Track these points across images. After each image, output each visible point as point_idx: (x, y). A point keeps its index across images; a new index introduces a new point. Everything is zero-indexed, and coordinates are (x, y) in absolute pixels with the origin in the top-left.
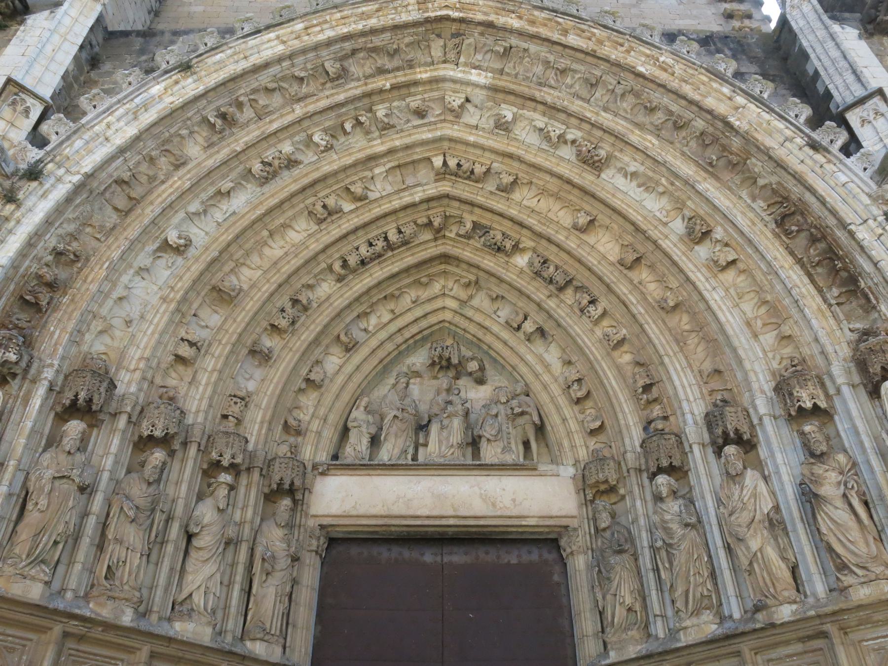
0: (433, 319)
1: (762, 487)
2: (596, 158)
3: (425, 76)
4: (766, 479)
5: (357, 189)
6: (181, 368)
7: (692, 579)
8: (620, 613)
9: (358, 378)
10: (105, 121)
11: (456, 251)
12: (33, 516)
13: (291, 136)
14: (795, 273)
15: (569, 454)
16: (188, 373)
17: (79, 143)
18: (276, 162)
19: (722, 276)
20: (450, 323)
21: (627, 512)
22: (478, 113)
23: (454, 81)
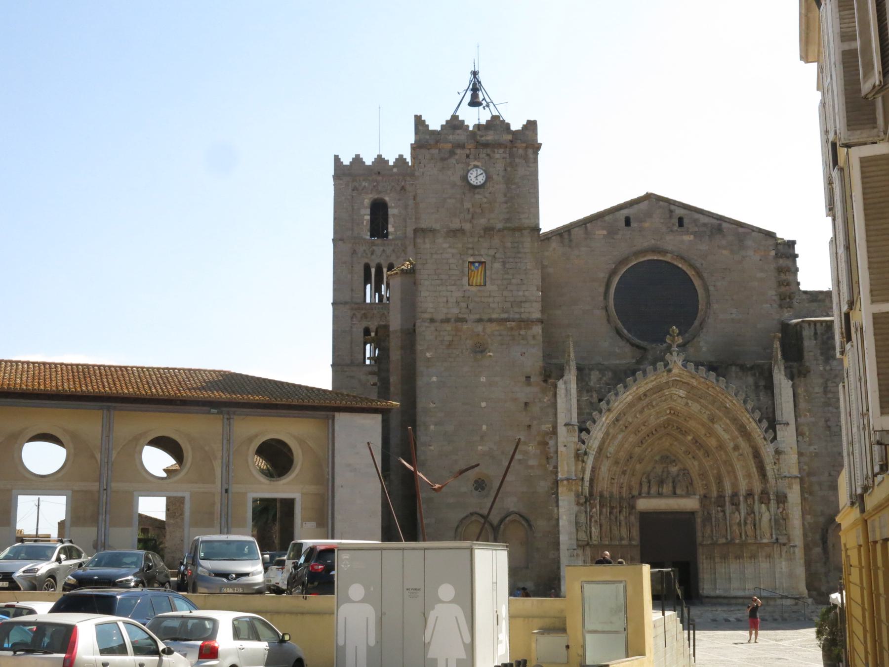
1: (738, 516)
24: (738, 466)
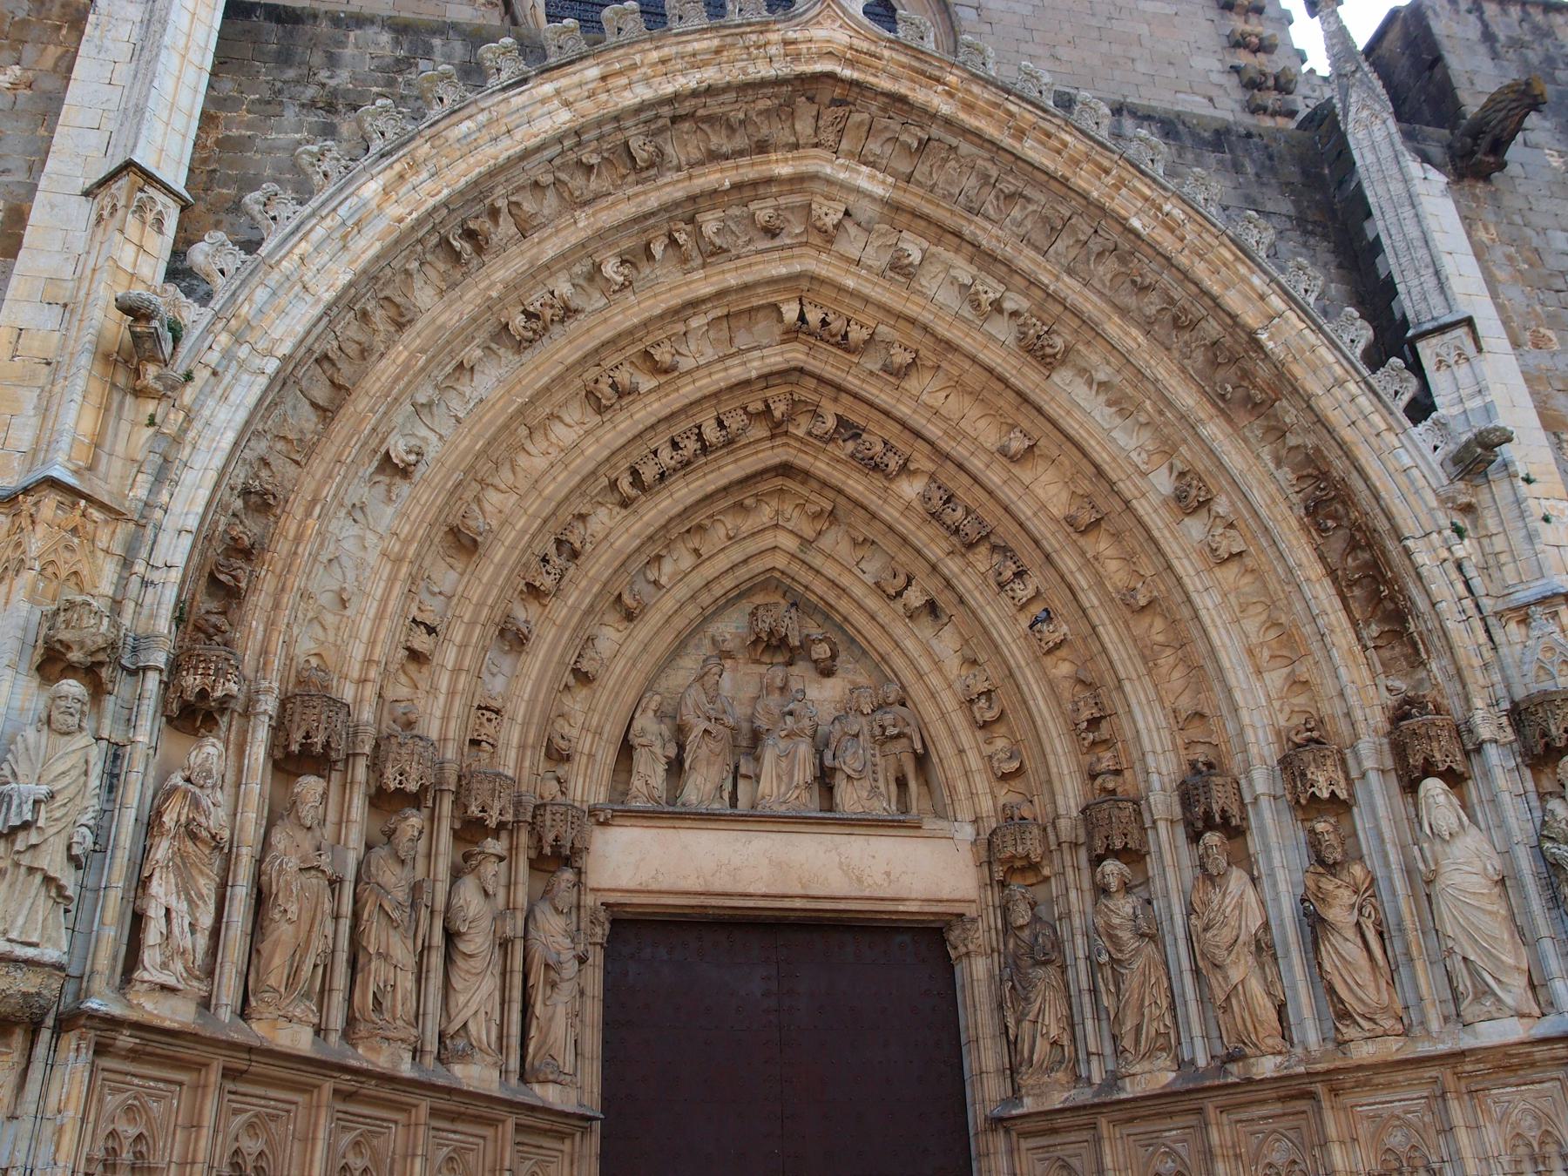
0: (758, 566)
2: (1049, 351)
3: (784, 170)
4: (1254, 881)
5: (663, 355)
6: (412, 668)
7: (1146, 1011)
8: (1042, 1047)
9: (647, 663)
10: (297, 251)
11: (803, 461)
12: (283, 932)
13: (568, 268)
14: (1324, 588)
15: (966, 804)
16: (422, 675)
17: (261, 295)
18: (548, 313)
19: (1218, 572)
20: (783, 573)
21: (1051, 901)
22: (863, 237)
23: (829, 182)
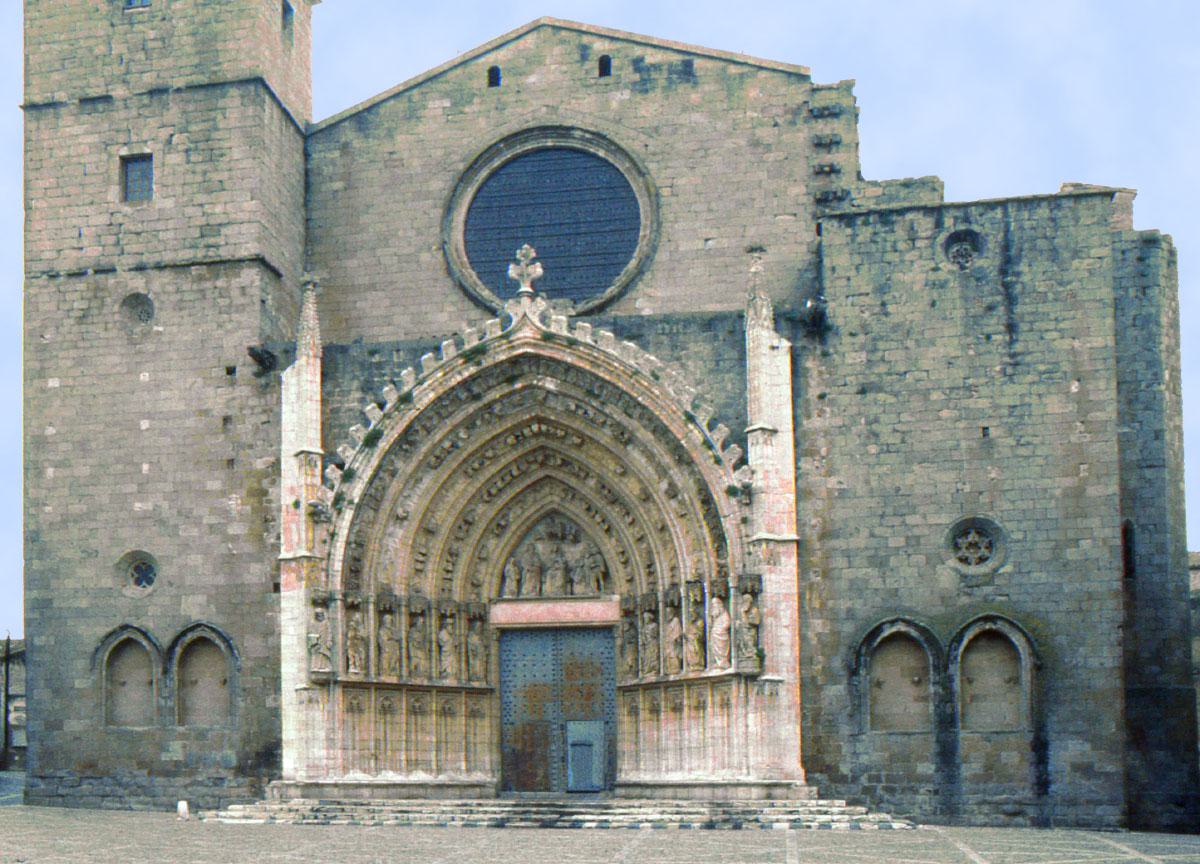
1: (677, 628)
24: (677, 528)
